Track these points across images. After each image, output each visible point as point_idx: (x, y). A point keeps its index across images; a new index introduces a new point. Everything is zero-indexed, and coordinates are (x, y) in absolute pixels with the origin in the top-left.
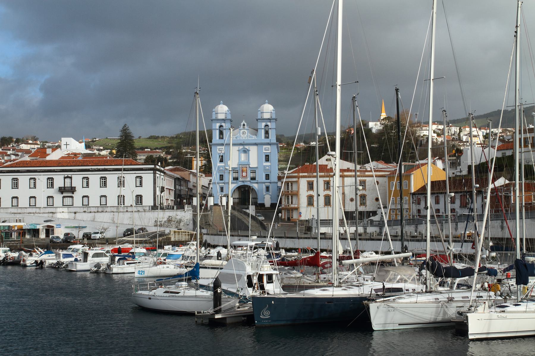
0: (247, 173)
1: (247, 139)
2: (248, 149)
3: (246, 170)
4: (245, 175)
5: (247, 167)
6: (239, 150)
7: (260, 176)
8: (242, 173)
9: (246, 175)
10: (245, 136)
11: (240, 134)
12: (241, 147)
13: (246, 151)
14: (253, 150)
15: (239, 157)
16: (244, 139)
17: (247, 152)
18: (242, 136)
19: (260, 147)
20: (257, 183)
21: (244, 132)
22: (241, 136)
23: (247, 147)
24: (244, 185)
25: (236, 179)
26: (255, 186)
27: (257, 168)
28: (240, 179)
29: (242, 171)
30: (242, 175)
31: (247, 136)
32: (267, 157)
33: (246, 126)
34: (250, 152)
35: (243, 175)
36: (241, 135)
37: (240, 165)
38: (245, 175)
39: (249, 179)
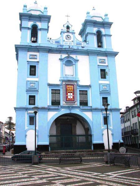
0: (73, 94)
1: (73, 45)
2: (75, 58)
3: (73, 89)
4: (72, 97)
5: (73, 85)
6: (61, 59)
7: (94, 100)
8: (67, 94)
9: (73, 97)
10: (71, 41)
11: (63, 38)
12: (64, 56)
13: (69, 63)
14: (83, 62)
15: (62, 71)
16: (68, 44)
17: (74, 63)
18: (66, 40)
19: (92, 57)
20: (91, 110)
21: (69, 37)
22: (64, 41)
23: (74, 56)
24: (71, 113)
25: (56, 103)
26: (88, 116)
27: (89, 86)
28: (62, 103)
29: (67, 92)
30: (67, 97)
31: (73, 41)
32: (103, 73)
33: (70, 29)
34: (79, 64)
35: (69, 97)
36: (64, 39)
37: (63, 81)
38: (72, 97)
39: (78, 103)
